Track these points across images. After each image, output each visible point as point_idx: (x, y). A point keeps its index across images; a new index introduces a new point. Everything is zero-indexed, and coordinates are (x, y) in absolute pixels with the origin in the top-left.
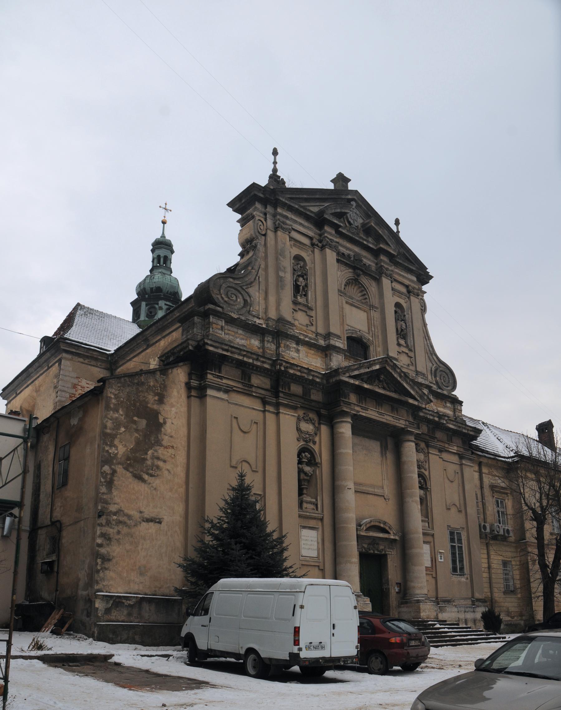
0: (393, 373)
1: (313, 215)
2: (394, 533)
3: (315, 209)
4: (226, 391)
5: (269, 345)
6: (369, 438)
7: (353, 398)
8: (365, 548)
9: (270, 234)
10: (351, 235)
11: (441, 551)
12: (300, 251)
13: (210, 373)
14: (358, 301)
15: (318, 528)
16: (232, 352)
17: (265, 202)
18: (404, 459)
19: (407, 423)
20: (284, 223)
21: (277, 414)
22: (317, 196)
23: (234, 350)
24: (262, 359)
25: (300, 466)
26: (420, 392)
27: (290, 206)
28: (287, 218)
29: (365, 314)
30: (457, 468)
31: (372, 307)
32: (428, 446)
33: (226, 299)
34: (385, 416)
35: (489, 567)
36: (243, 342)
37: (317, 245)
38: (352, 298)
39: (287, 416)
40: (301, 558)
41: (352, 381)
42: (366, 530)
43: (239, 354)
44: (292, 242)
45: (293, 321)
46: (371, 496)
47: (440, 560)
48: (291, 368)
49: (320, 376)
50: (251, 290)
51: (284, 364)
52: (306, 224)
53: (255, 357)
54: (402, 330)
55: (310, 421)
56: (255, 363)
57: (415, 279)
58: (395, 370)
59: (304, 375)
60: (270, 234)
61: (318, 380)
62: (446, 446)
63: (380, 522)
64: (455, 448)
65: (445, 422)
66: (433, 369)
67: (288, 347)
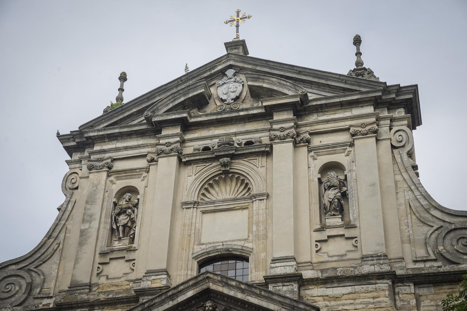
0: (226, 291)
1: (143, 127)
10: (214, 117)
12: (127, 181)
14: (224, 201)
17: (80, 148)
27: (108, 135)
28: (104, 151)
29: (246, 212)
31: (255, 196)
37: (152, 160)
38: (214, 202)
44: (112, 178)
50: (45, 268)
52: (141, 142)
54: (330, 202)
57: (369, 110)
58: (227, 285)
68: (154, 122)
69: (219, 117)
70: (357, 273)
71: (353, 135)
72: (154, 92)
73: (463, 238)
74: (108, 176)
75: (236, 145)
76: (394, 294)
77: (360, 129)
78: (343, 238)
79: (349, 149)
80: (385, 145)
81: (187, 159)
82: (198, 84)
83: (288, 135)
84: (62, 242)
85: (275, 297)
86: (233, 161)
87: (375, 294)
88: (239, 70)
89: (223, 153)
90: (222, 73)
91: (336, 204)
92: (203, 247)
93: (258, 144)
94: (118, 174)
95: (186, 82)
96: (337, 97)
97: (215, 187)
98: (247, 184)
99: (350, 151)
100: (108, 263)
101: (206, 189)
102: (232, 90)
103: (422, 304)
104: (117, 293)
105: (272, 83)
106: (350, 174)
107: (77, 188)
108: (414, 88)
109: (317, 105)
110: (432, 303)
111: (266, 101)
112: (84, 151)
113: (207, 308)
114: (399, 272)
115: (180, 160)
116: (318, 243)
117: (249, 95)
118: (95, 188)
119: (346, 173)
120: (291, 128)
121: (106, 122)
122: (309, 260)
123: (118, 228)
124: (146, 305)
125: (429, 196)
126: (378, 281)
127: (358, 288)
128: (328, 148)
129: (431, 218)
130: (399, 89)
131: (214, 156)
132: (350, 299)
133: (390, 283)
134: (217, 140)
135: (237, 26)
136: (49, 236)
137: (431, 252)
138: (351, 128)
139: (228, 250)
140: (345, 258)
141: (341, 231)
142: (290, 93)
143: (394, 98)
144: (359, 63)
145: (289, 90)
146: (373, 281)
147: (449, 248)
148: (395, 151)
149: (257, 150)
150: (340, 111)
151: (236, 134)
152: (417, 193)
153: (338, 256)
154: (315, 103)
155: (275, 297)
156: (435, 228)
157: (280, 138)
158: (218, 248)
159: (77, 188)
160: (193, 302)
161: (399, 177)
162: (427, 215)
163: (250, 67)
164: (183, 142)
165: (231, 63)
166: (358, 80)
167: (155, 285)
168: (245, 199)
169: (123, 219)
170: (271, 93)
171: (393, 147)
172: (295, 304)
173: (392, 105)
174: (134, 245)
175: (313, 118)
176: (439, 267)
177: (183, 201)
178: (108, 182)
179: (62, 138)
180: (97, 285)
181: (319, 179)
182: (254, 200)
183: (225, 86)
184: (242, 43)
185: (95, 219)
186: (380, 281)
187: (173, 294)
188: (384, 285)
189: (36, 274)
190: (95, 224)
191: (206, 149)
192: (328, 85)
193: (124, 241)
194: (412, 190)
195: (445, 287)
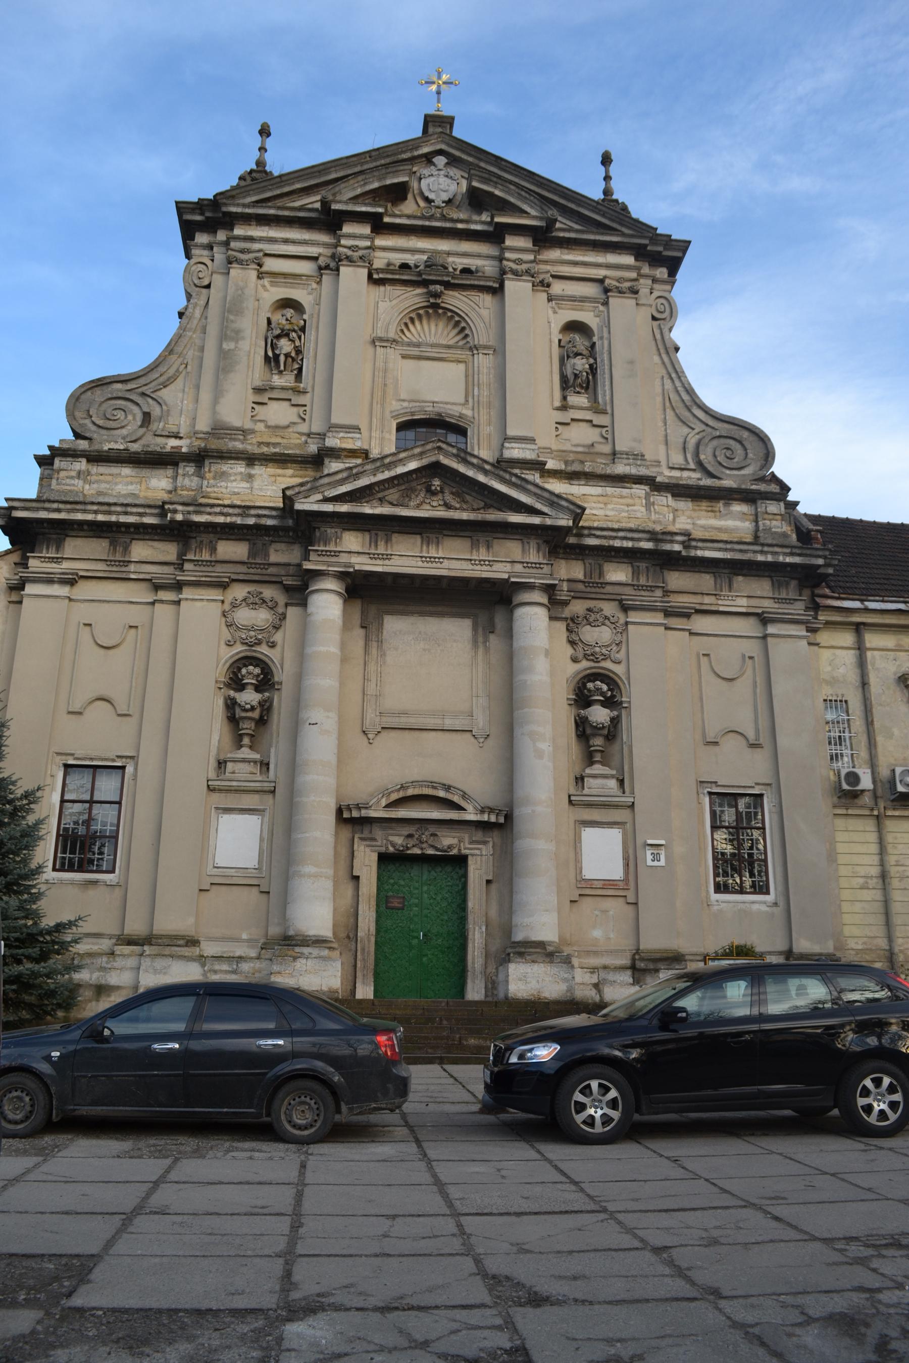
0: (462, 469)
2: (475, 808)
3: (313, 201)
4: (72, 582)
5: (187, 482)
6: (441, 615)
7: (352, 541)
8: (393, 845)
9: (218, 280)
11: (650, 842)
13: (34, 557)
14: (433, 346)
15: (264, 811)
16: (69, 511)
17: (210, 226)
18: (515, 645)
19: (518, 568)
20: (249, 251)
21: (178, 603)
22: (333, 176)
23: (69, 506)
24: (134, 510)
25: (232, 693)
26: (546, 495)
28: (251, 239)
29: (462, 367)
30: (752, 648)
32: (625, 609)
33: (100, 422)
34: (454, 560)
35: (884, 876)
36: (132, 488)
37: (327, 267)
38: (418, 345)
39: (198, 604)
40: (211, 870)
41: (329, 508)
42: (386, 806)
43: (85, 511)
44: (266, 281)
45: (248, 425)
46: (433, 734)
47: (649, 863)
48: (197, 513)
49: (274, 513)
50: (165, 394)
51: (180, 508)
52: (306, 235)
53: (119, 509)
54: (576, 376)
55: (259, 602)
56: (123, 519)
57: (629, 260)
58: (465, 461)
59: (234, 519)
60: (218, 280)
61: (270, 522)
62: (707, 600)
63: (434, 788)
64: (744, 602)
65: (677, 547)
66: (692, 442)
67: (222, 475)
68: (334, 210)
69: (427, 223)
70: (609, 471)
71: (606, 291)
72: (329, 165)
73: (728, 449)
74: (258, 277)
75: (451, 270)
76: (649, 505)
77: (617, 284)
78: (589, 424)
79: (601, 308)
80: (644, 314)
81: (381, 276)
82: (402, 168)
83: (528, 272)
84: (190, 363)
85: (530, 487)
86: (446, 292)
87: (630, 501)
88: (453, 161)
89: (434, 278)
90: (428, 159)
91: (584, 378)
92: (405, 404)
93: (480, 274)
94: (274, 277)
95: (375, 160)
96: (593, 233)
97: (417, 323)
98: (463, 329)
99: (603, 312)
100: (266, 404)
101: (406, 324)
102: (442, 187)
103: (678, 520)
104: (286, 448)
105: (508, 192)
106: (600, 342)
107: (208, 287)
108: (686, 244)
109: (564, 237)
110: (689, 521)
111: (500, 215)
112: (216, 232)
113: (433, 488)
114: (659, 479)
115: (370, 276)
116: (558, 426)
117: (467, 202)
118: (240, 292)
119: (595, 339)
120: (531, 262)
121: (255, 195)
122: (548, 446)
123: (276, 357)
124: (354, 471)
125: (693, 390)
126: (634, 486)
127: (610, 490)
128: (575, 301)
129: (691, 418)
130: (667, 241)
131: (419, 279)
132: (599, 502)
133: (648, 490)
134: (425, 257)
135: (438, 93)
136: (170, 350)
137: (690, 460)
138: (607, 281)
139: (440, 414)
140: (592, 450)
141: (588, 415)
142: (533, 212)
143: (661, 252)
144: (607, 192)
145: (532, 207)
146: (628, 485)
147: (711, 458)
148: (656, 323)
149: (482, 283)
150: (591, 253)
151: (449, 254)
152: (678, 384)
153: (584, 446)
154: (561, 234)
155: (530, 487)
156: (696, 431)
157: (515, 273)
158: (427, 409)
159: (208, 287)
160: (414, 476)
161: (656, 359)
162: (687, 414)
163: (470, 159)
164: (372, 248)
165: (443, 147)
166: (621, 217)
167: (344, 446)
168: (462, 348)
169: (285, 346)
170: (504, 206)
171: (654, 318)
172: (555, 499)
173: (656, 260)
174: (302, 385)
175: (555, 254)
176: (699, 479)
177: (375, 335)
178: (259, 286)
179: (182, 208)
180: (253, 432)
181: (560, 341)
182: (475, 352)
183: (432, 179)
184: (450, 120)
185: (243, 338)
186: (637, 486)
187: (390, 463)
188: (640, 491)
189: (154, 403)
190: (245, 345)
191: (405, 266)
192: (579, 212)
193: (287, 377)
194: (671, 379)
195: (704, 504)
